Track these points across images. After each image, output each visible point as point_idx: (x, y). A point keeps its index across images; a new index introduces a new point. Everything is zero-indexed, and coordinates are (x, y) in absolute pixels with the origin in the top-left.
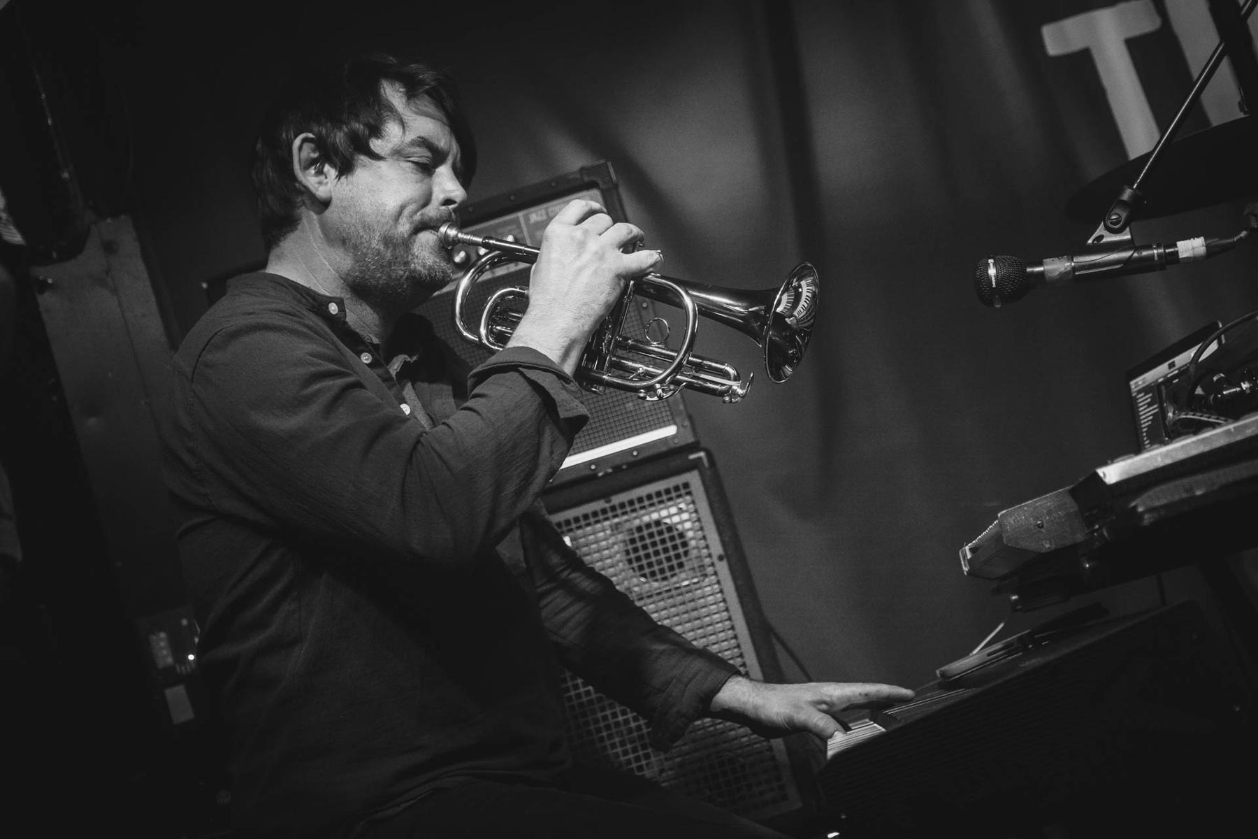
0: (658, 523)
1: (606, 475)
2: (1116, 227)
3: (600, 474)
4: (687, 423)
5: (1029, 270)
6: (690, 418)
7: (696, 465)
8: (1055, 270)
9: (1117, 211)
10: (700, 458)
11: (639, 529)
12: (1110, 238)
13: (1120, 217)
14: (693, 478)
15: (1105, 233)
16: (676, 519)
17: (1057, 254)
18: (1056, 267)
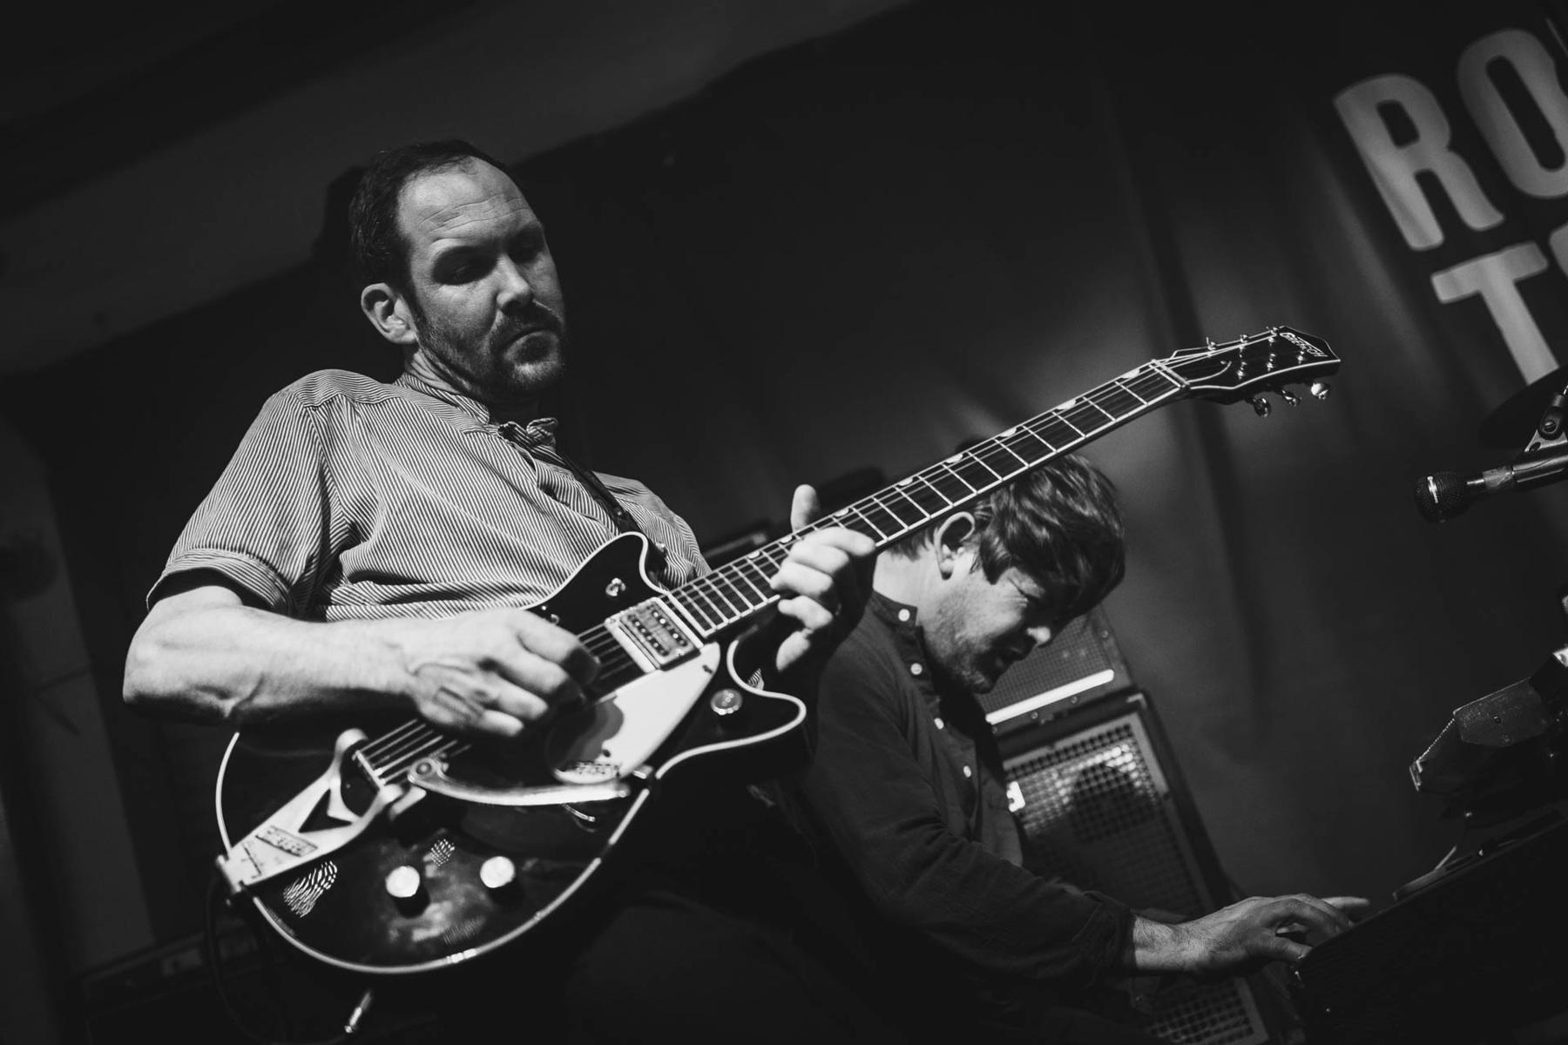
0: (1102, 765)
1: (1048, 723)
2: (1552, 433)
3: (1043, 721)
4: (1122, 667)
5: (1469, 483)
6: (1125, 662)
7: (1134, 707)
8: (1495, 480)
9: (1550, 418)
10: (1137, 702)
11: (1084, 772)
12: (1546, 445)
13: (1554, 423)
14: (1133, 720)
15: (1541, 440)
16: (1119, 762)
17: (1497, 465)
18: (1496, 477)
